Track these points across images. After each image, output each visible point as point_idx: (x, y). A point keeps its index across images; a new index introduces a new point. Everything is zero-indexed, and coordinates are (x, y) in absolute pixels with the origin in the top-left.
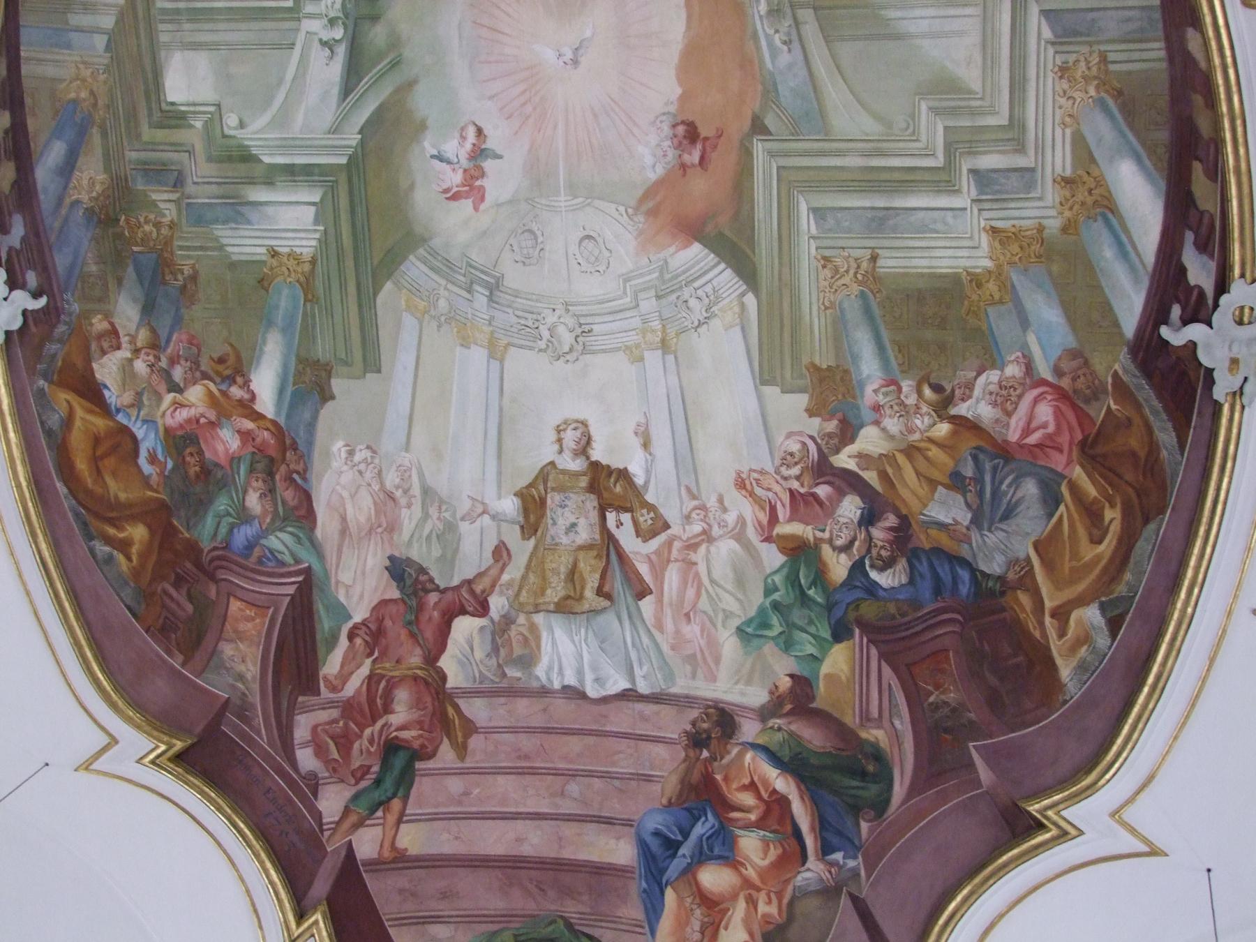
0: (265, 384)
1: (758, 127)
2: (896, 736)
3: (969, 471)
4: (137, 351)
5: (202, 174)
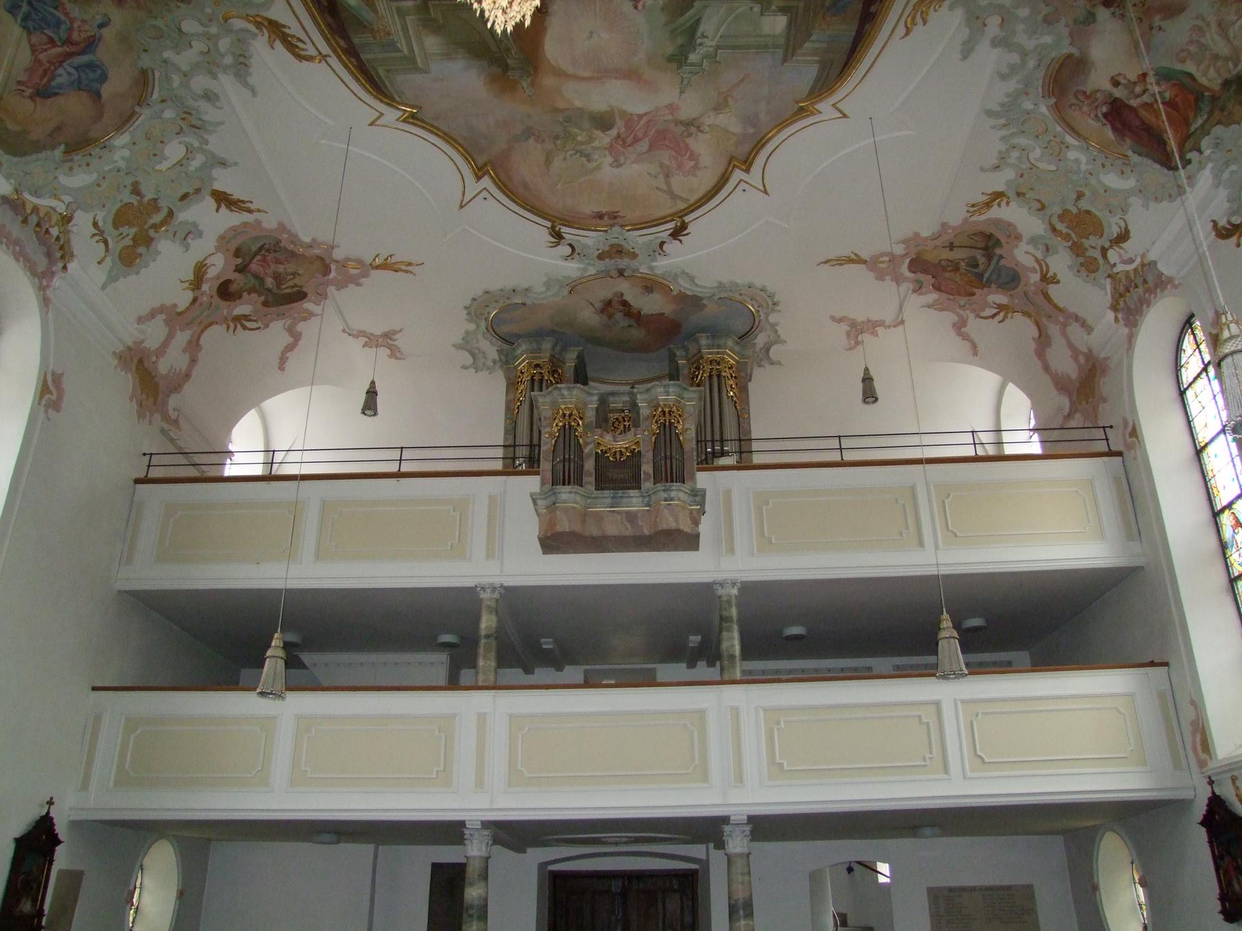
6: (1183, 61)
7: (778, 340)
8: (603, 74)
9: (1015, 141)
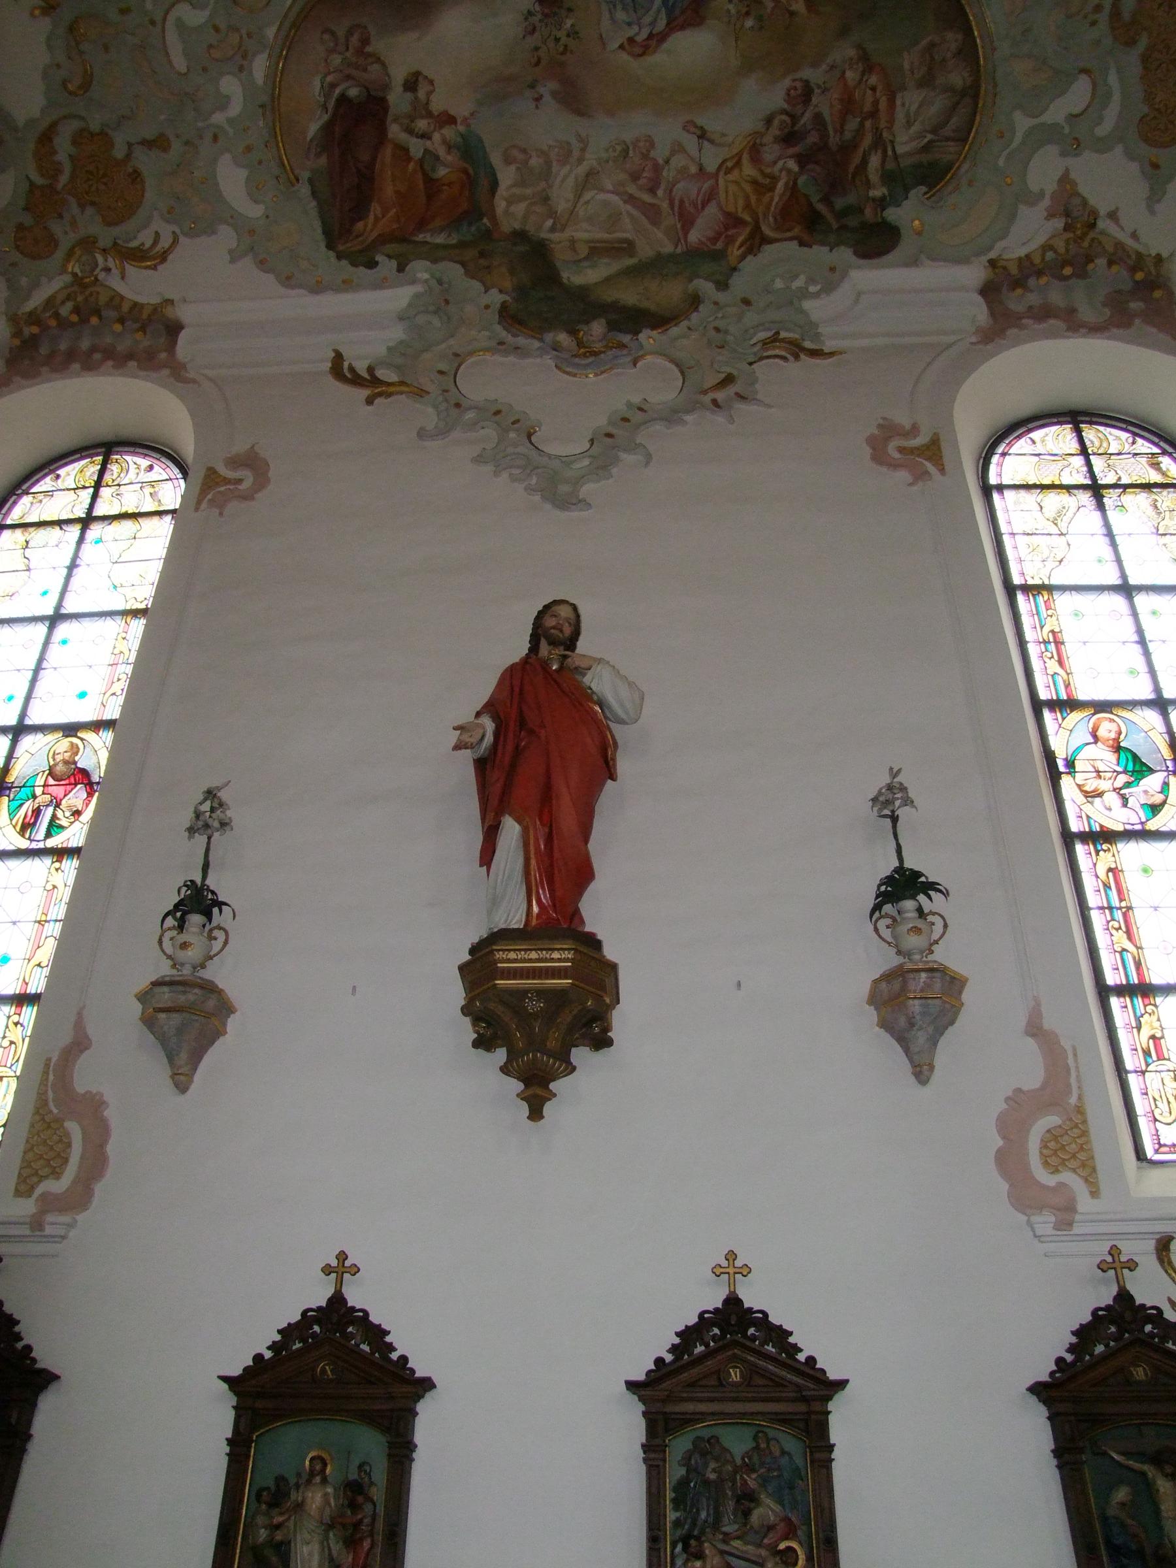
6: (508, 161)
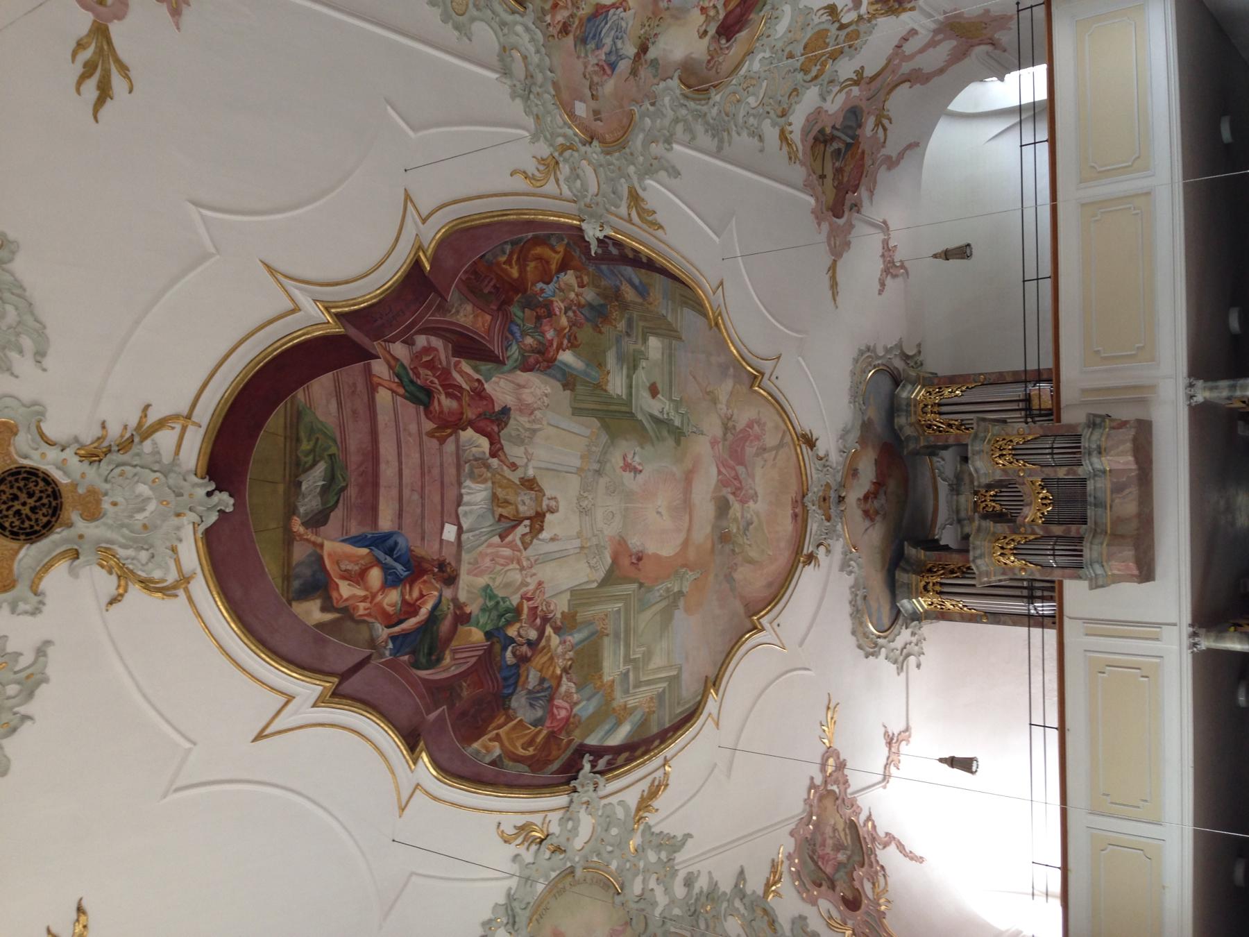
0: (567, 357)
1: (641, 585)
2: (447, 669)
3: (546, 685)
4: (577, 295)
5: (630, 345)
7: (899, 346)
8: (686, 505)
9: (741, 121)
